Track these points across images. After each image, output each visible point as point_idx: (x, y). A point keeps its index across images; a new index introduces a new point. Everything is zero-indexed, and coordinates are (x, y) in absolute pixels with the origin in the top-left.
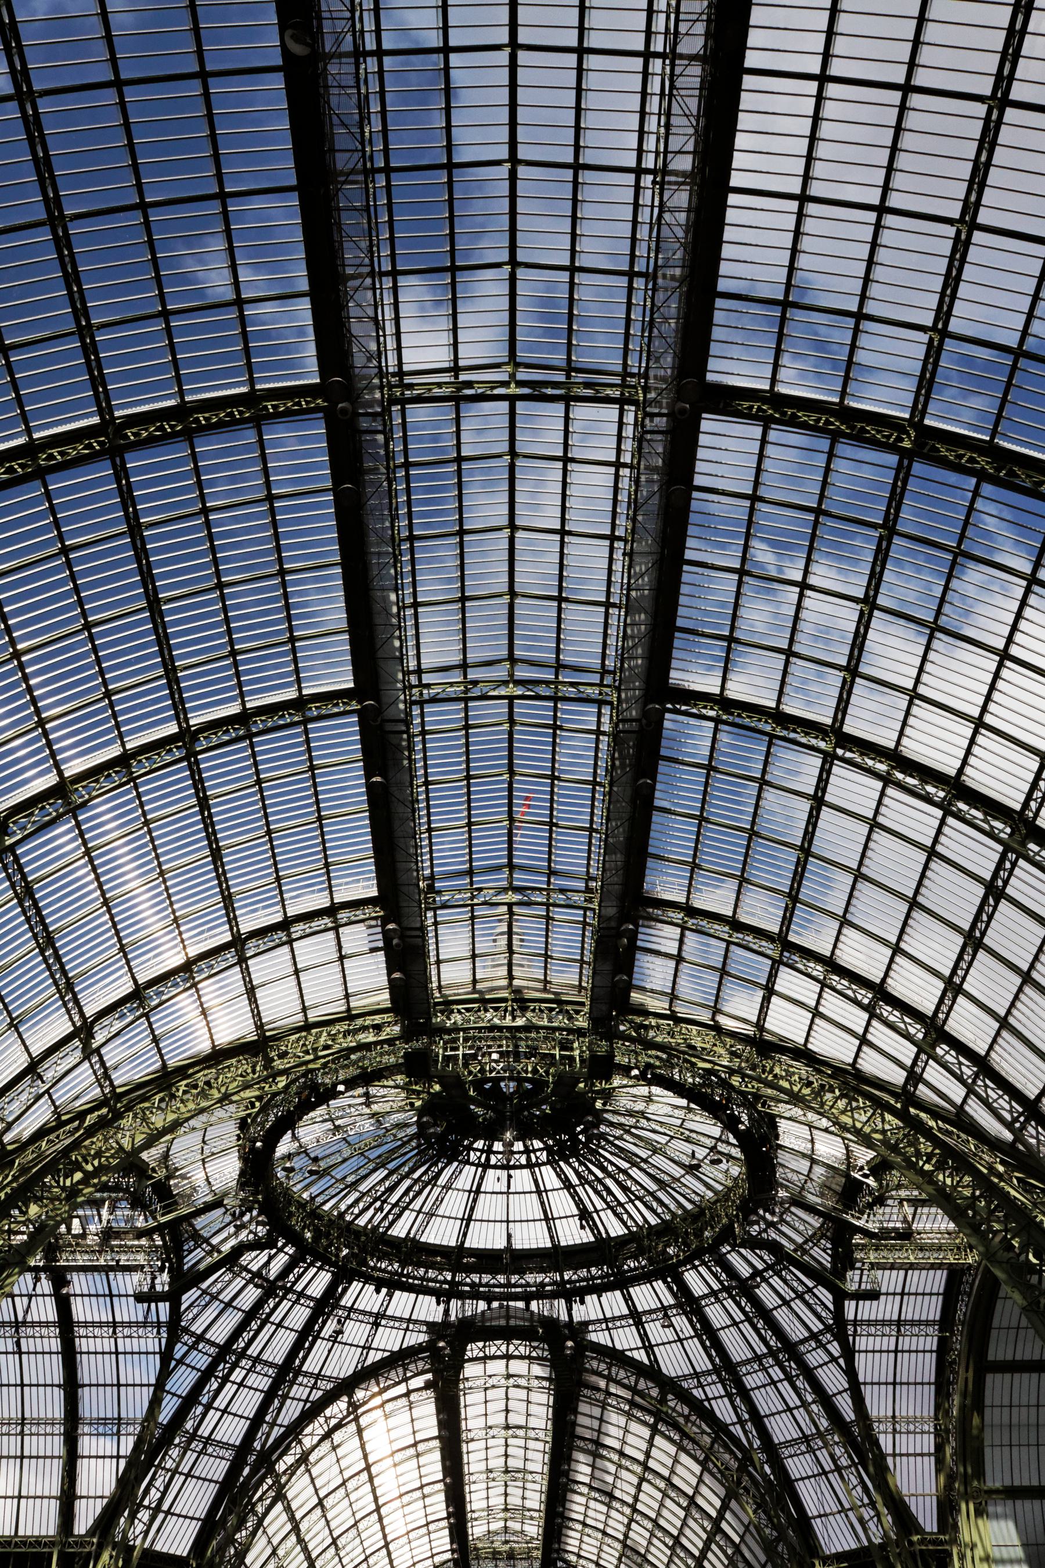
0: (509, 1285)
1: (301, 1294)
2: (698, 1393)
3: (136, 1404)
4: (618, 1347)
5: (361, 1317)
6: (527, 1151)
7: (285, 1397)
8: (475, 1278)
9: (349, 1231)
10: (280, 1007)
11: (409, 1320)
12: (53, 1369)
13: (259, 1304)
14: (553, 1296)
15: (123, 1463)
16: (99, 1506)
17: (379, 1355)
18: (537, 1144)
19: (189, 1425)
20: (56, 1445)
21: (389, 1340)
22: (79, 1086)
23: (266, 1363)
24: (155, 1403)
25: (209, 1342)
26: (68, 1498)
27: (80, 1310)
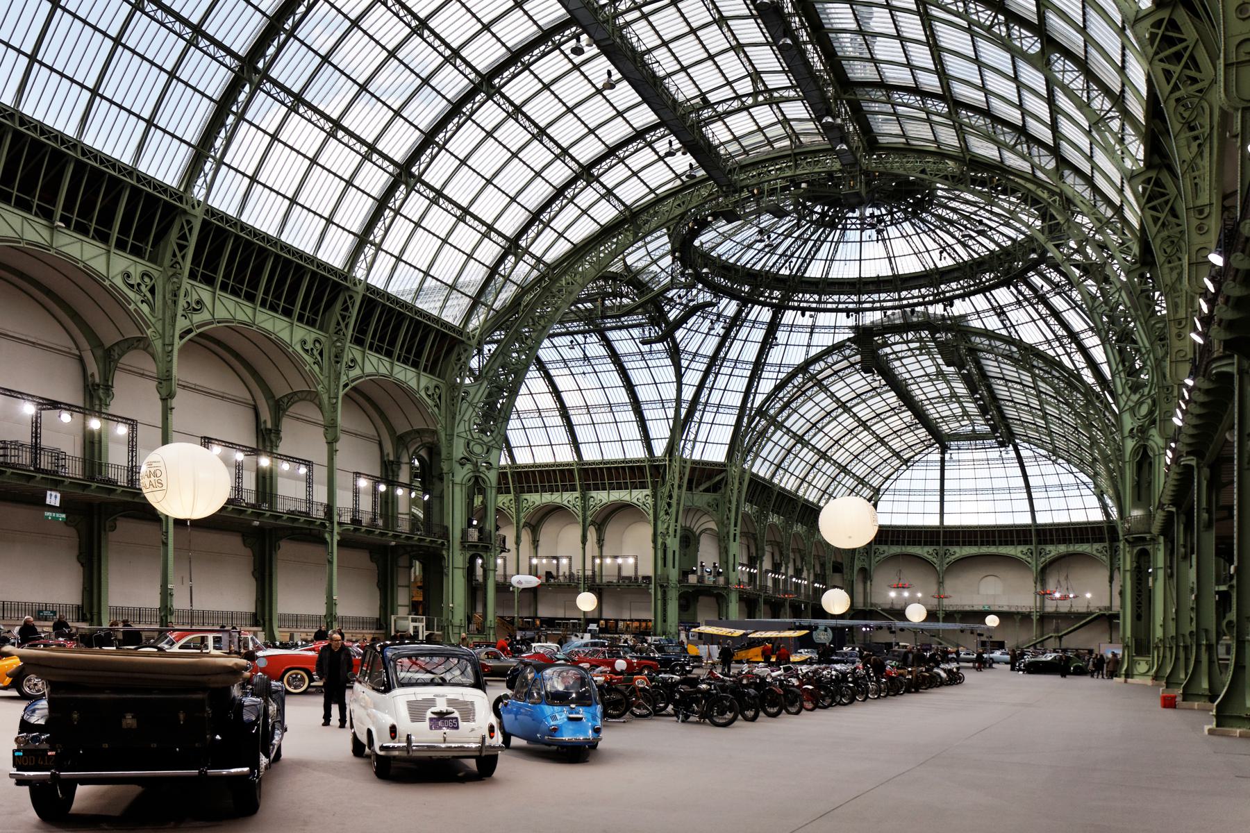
0: (900, 299)
1: (755, 322)
2: (1051, 353)
3: (670, 392)
4: (989, 328)
7: (760, 378)
9: (774, 280)
10: (632, 193)
11: (835, 327)
12: (614, 379)
13: (728, 330)
14: (931, 303)
15: (671, 422)
16: (665, 443)
17: (820, 349)
19: (703, 400)
20: (631, 416)
21: (823, 340)
22: (522, 270)
23: (743, 362)
24: (679, 391)
25: (702, 356)
26: (647, 440)
27: (621, 348)
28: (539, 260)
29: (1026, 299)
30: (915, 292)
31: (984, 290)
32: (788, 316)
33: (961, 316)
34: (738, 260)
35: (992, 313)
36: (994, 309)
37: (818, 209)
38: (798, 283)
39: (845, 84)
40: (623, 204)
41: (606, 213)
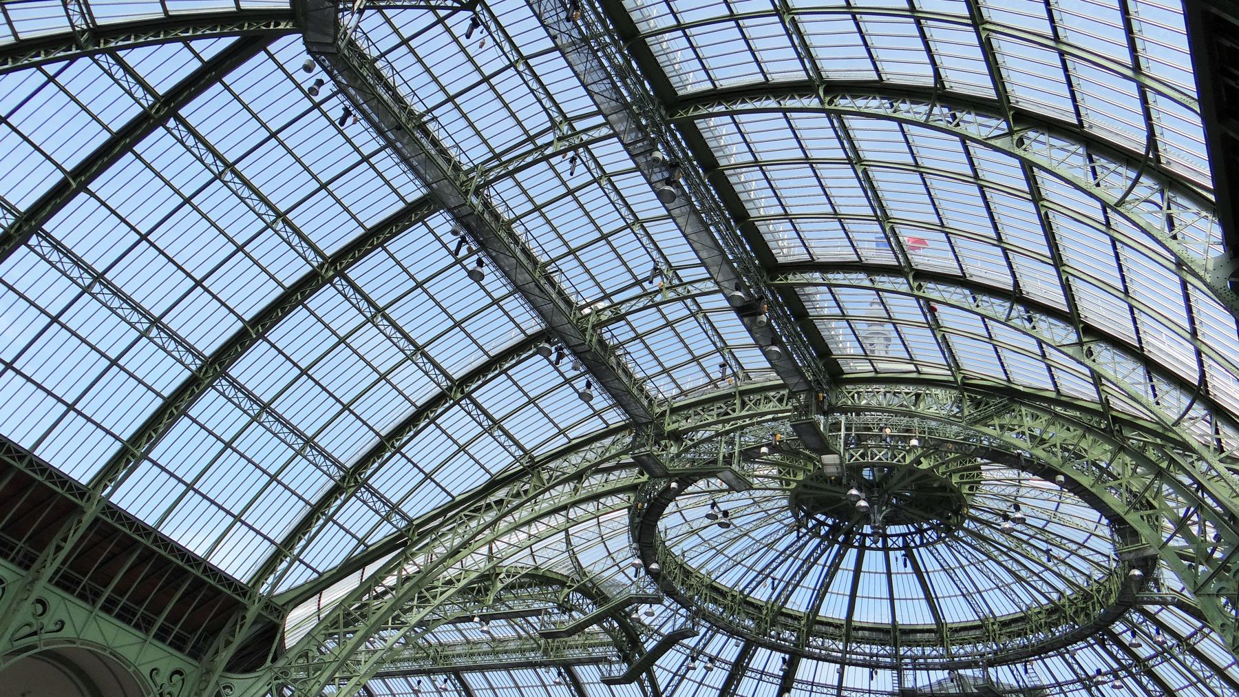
5: (825, 690)
6: (921, 532)
8: (917, 651)
10: (533, 433)
14: (991, 664)
18: (925, 526)
28: (395, 508)
29: (1123, 667)
30: (968, 648)
31: (1059, 646)
32: (806, 668)
33: (1035, 688)
34: (736, 584)
35: (1078, 686)
36: (1080, 680)
37: (830, 522)
38: (812, 623)
39: (771, 267)
40: (521, 447)
41: (499, 460)
